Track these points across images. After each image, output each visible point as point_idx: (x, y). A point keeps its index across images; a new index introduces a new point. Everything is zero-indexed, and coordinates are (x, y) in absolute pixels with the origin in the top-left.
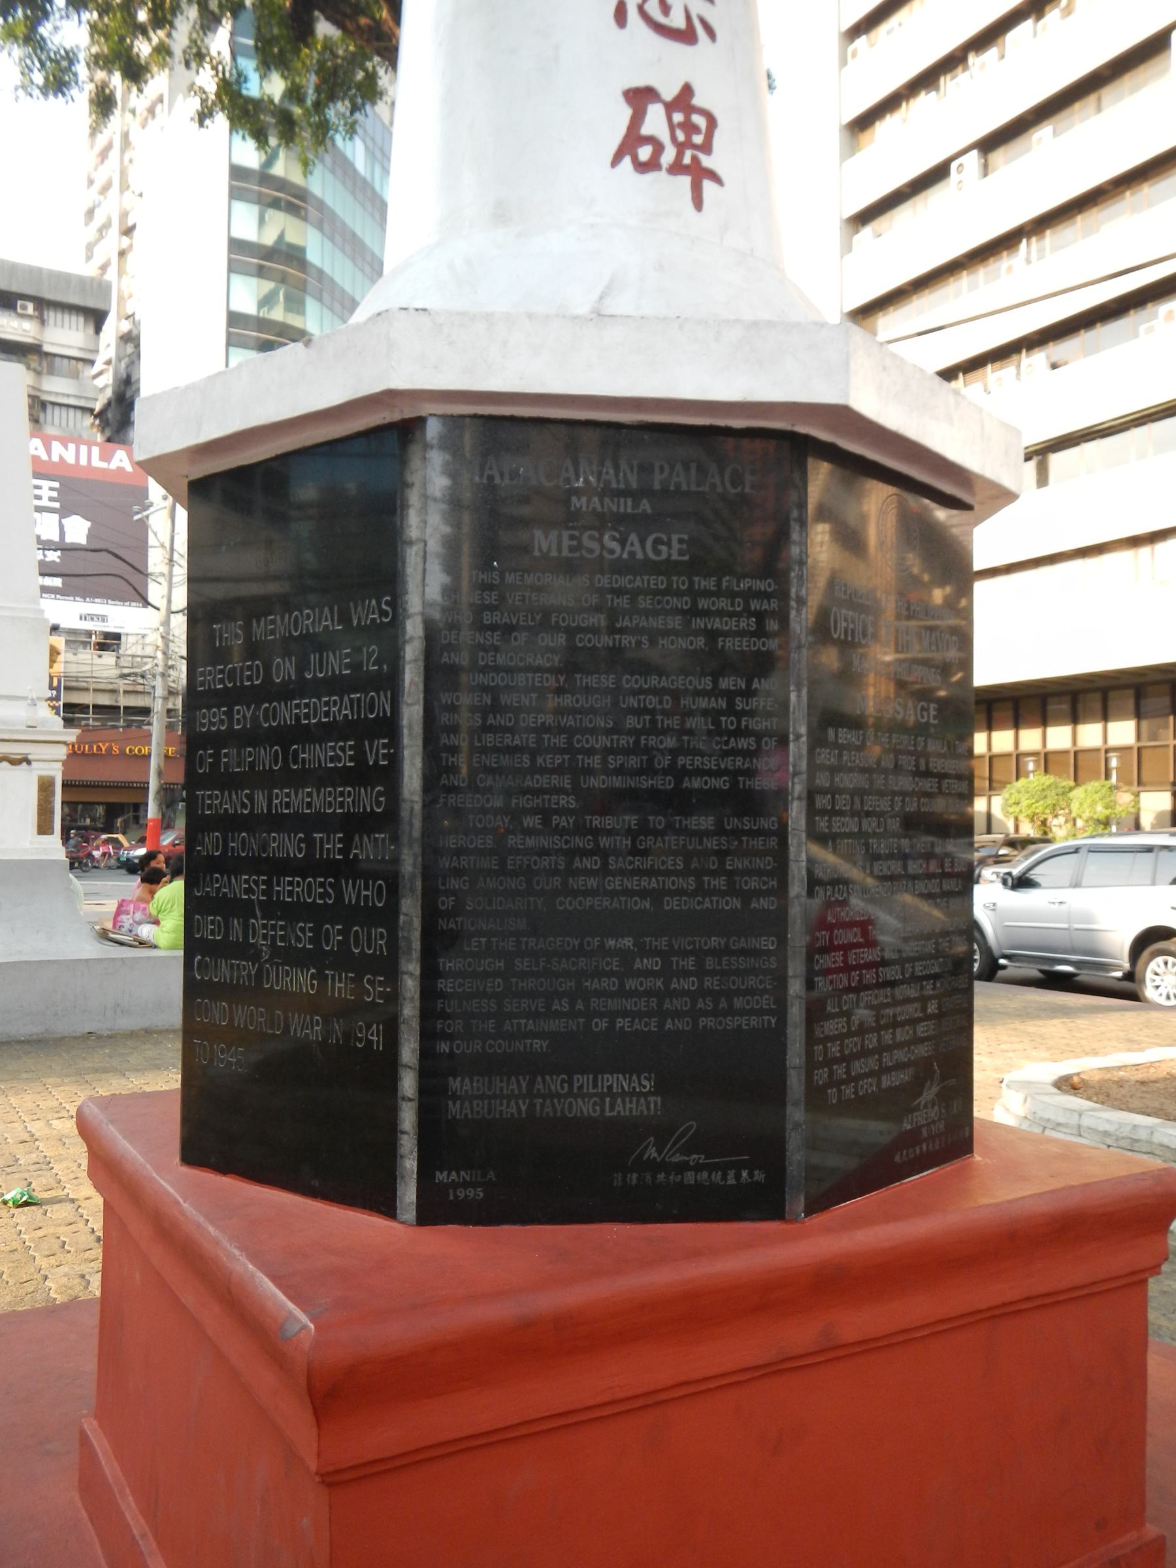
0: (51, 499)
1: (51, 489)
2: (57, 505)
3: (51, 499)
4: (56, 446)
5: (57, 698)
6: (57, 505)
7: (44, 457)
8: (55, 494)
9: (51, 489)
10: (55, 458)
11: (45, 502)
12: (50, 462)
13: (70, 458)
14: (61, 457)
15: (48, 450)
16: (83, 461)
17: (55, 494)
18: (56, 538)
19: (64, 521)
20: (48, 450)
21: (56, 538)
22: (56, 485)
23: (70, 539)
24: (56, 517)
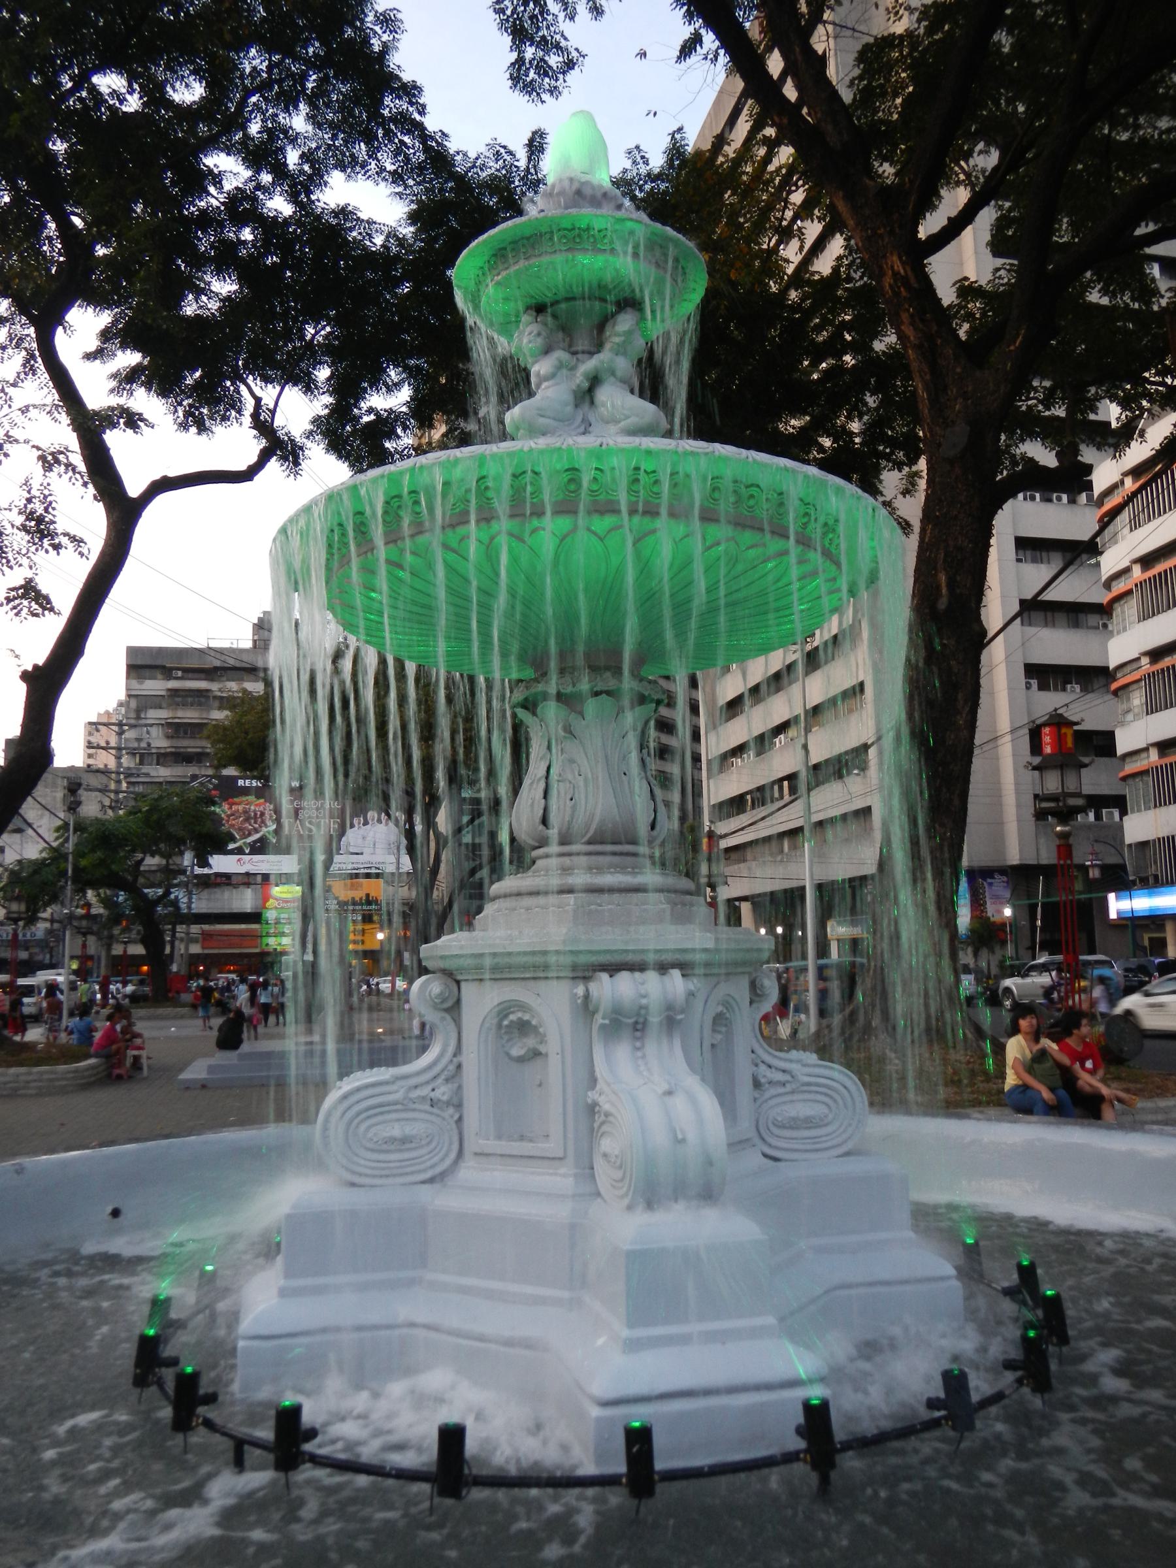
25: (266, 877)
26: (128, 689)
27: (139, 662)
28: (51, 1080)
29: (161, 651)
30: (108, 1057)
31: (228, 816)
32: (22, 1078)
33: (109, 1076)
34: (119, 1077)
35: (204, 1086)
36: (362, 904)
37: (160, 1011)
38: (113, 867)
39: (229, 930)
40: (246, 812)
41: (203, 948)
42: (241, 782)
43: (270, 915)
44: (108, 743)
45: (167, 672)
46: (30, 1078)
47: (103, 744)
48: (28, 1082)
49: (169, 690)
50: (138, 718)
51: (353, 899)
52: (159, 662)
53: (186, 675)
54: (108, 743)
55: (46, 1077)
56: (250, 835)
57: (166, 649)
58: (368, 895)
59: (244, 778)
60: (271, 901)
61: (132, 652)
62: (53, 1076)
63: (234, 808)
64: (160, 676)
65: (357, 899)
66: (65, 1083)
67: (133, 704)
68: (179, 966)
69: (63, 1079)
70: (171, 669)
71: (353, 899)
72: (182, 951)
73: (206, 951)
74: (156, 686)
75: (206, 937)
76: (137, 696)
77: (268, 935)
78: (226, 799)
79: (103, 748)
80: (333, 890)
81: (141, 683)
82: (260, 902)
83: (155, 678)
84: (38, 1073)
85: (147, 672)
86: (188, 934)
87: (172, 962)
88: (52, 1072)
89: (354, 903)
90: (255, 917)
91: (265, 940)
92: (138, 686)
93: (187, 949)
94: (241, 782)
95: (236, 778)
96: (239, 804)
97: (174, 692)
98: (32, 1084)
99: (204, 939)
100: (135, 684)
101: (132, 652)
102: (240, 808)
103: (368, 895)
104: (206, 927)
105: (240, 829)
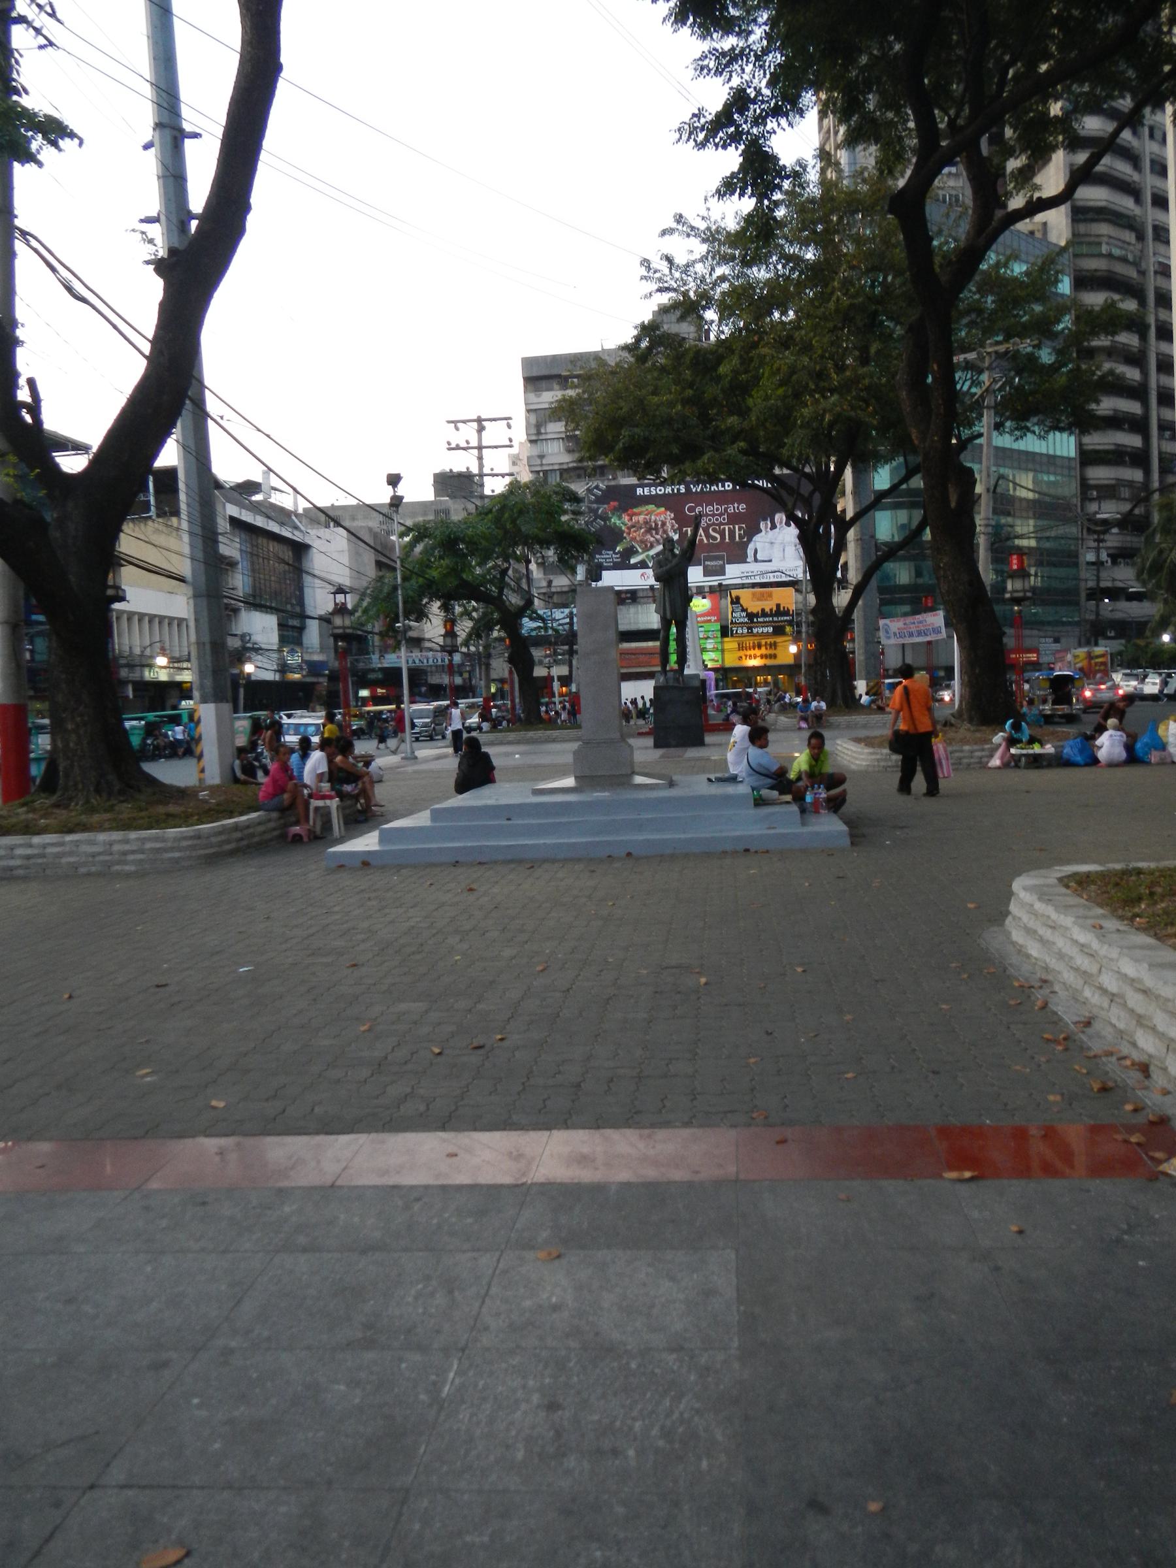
26: (526, 404)
27: (535, 374)
28: (158, 850)
29: (555, 359)
30: (283, 810)
31: (629, 528)
32: (116, 848)
33: (283, 837)
34: (298, 839)
35: (366, 864)
36: (771, 615)
37: (531, 734)
38: (464, 576)
39: (637, 648)
40: (646, 523)
42: (639, 491)
44: (468, 442)
46: (127, 847)
47: (463, 445)
48: (125, 853)
50: (539, 433)
51: (763, 610)
52: (555, 372)
54: (468, 442)
55: (148, 845)
56: (652, 546)
58: (778, 606)
59: (643, 486)
61: (528, 363)
62: (158, 845)
63: (635, 519)
64: (556, 386)
65: (767, 610)
66: (177, 855)
67: (533, 420)
69: (172, 849)
70: (566, 378)
71: (763, 610)
78: (625, 510)
79: (464, 449)
80: (742, 601)
81: (539, 396)
83: (550, 389)
84: (138, 839)
85: (544, 384)
88: (156, 839)
89: (764, 614)
94: (639, 491)
95: (634, 487)
96: (639, 514)
98: (131, 857)
100: (532, 396)
101: (528, 363)
102: (641, 518)
103: (778, 606)
105: (642, 542)
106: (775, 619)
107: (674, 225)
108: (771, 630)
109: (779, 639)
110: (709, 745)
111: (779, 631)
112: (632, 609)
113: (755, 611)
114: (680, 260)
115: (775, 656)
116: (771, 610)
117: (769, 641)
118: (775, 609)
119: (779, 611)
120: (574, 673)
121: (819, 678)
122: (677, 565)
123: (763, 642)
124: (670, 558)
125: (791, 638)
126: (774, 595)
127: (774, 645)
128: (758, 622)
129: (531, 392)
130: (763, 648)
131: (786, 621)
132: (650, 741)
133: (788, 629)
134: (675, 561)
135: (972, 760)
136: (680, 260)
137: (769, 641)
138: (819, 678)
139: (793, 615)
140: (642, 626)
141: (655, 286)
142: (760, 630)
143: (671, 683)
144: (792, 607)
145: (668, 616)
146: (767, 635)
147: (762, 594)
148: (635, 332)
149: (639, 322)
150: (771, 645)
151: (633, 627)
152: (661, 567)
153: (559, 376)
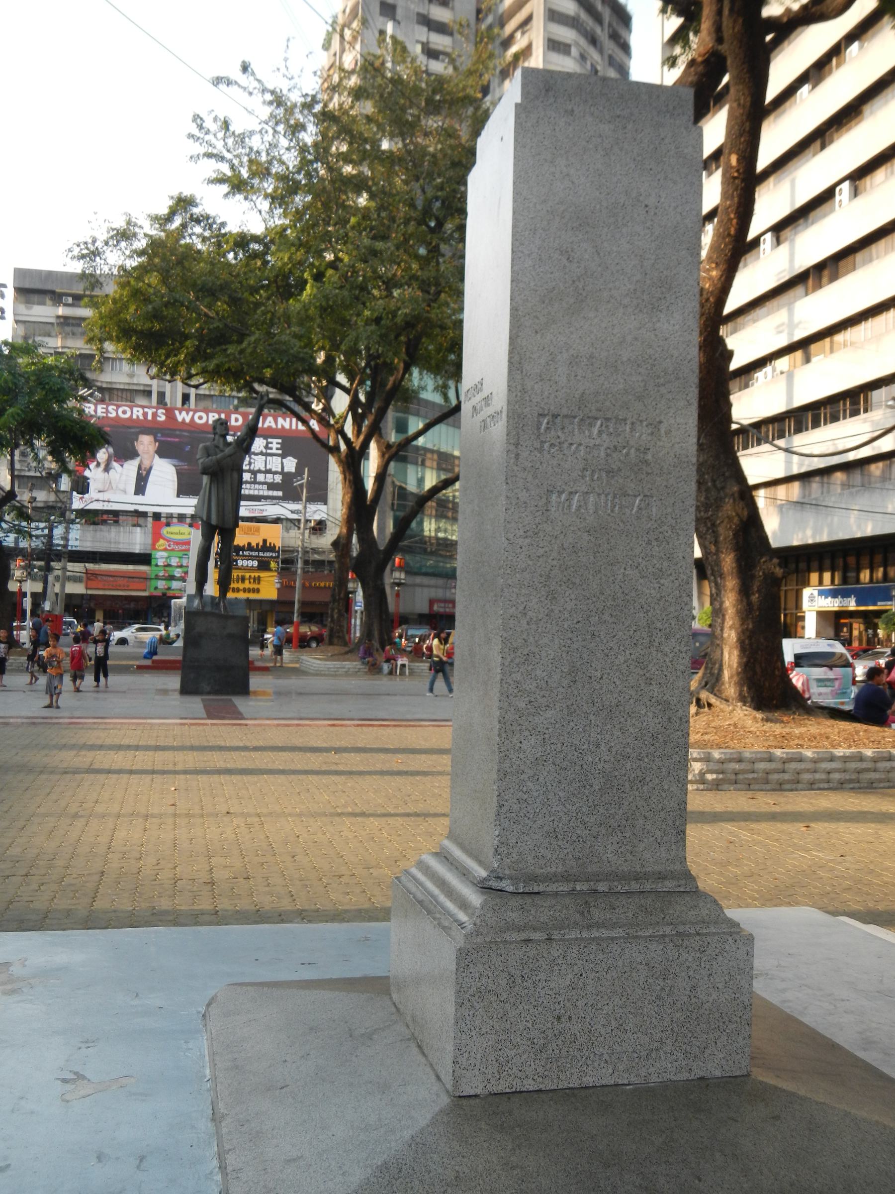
0: (277, 449)
1: (278, 443)
2: (280, 452)
3: (277, 449)
4: (280, 420)
5: (278, 557)
6: (280, 452)
7: (274, 426)
8: (279, 446)
9: (278, 443)
10: (279, 426)
11: (274, 451)
12: (277, 429)
13: (287, 426)
14: (285, 420)
15: (276, 422)
16: (294, 427)
17: (279, 446)
18: (280, 470)
19: (284, 460)
20: (276, 422)
21: (280, 470)
22: (280, 441)
23: (286, 470)
24: (279, 459)
25: (157, 516)
26: (15, 314)
27: (27, 286)
29: (50, 275)
36: (257, 550)
41: (87, 588)
43: (160, 557)
45: (57, 298)
49: (58, 317)
51: (249, 544)
52: (49, 287)
53: (76, 302)
57: (57, 272)
58: (265, 541)
60: (161, 541)
61: (20, 273)
64: (48, 302)
65: (254, 544)
68: (53, 604)
71: (249, 544)
72: (57, 589)
73: (90, 592)
74: (45, 312)
75: (90, 576)
76: (24, 322)
77: (157, 577)
82: (149, 541)
83: (44, 304)
85: (36, 298)
86: (64, 569)
87: (45, 599)
89: (250, 547)
90: (145, 559)
91: (154, 583)
92: (25, 311)
93: (63, 587)
97: (65, 321)
99: (88, 579)
100: (22, 308)
101: (20, 273)
103: (265, 541)
104: (90, 566)
106: (261, 554)
107: (236, 74)
108: (256, 563)
109: (263, 574)
110: (255, 693)
111: (264, 566)
112: (114, 529)
113: (241, 544)
114: (237, 127)
115: (258, 591)
116: (257, 545)
117: (253, 575)
118: (261, 544)
119: (266, 547)
120: (49, 590)
121: (336, 616)
122: (230, 456)
123: (247, 575)
124: (221, 446)
125: (276, 574)
126: (261, 530)
127: (258, 580)
128: (243, 556)
129: (21, 303)
130: (247, 582)
131: (272, 557)
132: (174, 681)
133: (273, 565)
134: (227, 451)
135: (818, 776)
136: (237, 127)
137: (253, 575)
138: (336, 616)
139: (278, 552)
140: (123, 548)
141: (202, 150)
142: (245, 563)
143: (208, 609)
144: (278, 544)
145: (214, 521)
146: (251, 569)
147: (250, 529)
148: (171, 203)
149: (175, 194)
150: (254, 579)
151: (113, 548)
152: (209, 456)
153: (53, 292)
